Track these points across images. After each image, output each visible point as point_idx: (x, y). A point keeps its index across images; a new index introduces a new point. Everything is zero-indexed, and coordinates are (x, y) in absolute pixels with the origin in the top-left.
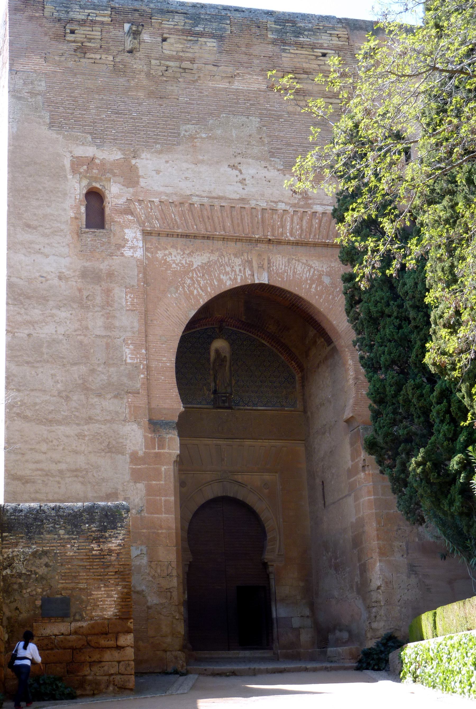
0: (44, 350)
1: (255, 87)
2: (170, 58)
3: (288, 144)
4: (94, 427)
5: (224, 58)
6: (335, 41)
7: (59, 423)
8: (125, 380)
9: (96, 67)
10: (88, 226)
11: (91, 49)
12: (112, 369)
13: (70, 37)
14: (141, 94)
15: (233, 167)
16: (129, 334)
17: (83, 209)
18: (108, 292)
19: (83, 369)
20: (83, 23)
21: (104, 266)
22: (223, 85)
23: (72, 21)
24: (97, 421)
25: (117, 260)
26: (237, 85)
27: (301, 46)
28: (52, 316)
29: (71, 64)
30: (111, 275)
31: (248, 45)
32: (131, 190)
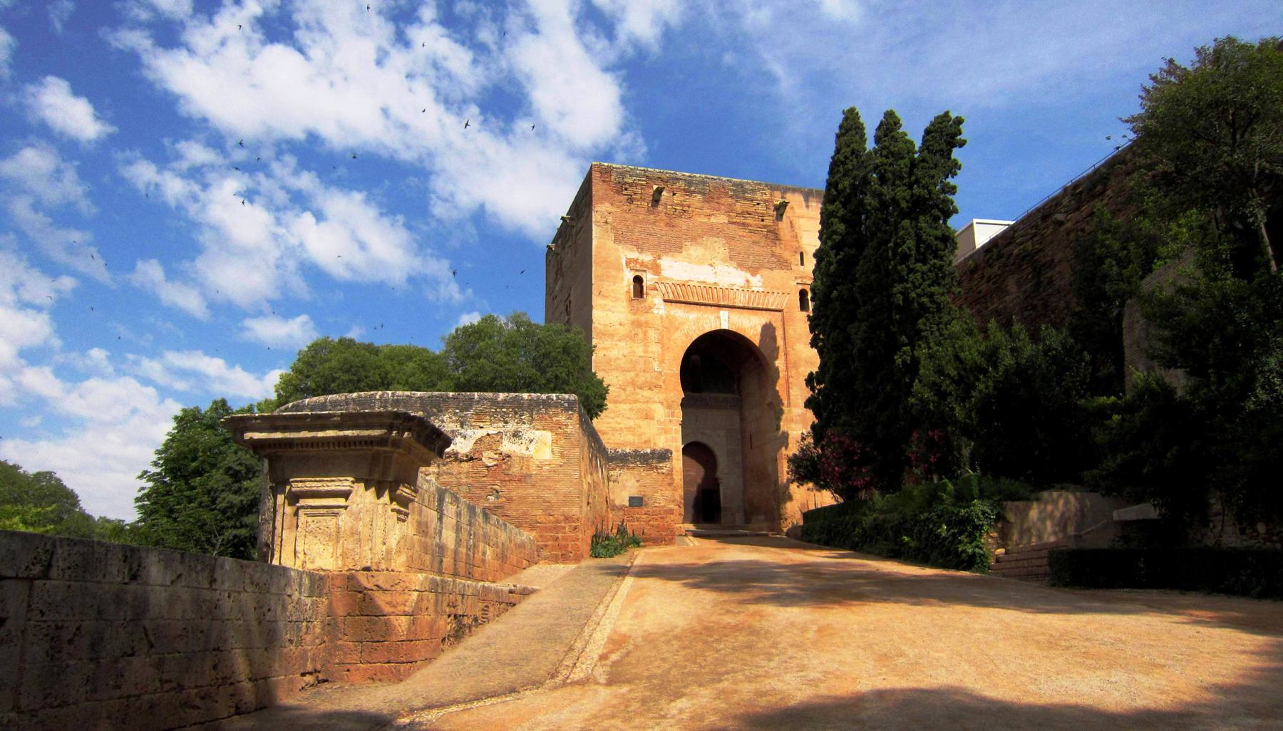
0: (613, 363)
1: (722, 221)
2: (678, 205)
3: (739, 254)
4: (638, 405)
5: (706, 205)
6: (764, 197)
7: (620, 402)
8: (654, 380)
9: (639, 209)
10: (634, 297)
11: (636, 199)
12: (648, 374)
13: (625, 192)
14: (662, 224)
15: (711, 265)
16: (656, 355)
17: (632, 287)
18: (645, 333)
19: (633, 374)
20: (631, 185)
21: (643, 318)
22: (705, 220)
23: (626, 183)
24: (640, 402)
25: (650, 316)
26: (713, 220)
27: (745, 199)
28: (616, 345)
29: (625, 207)
30: (647, 323)
31: (718, 198)
32: (656, 277)
